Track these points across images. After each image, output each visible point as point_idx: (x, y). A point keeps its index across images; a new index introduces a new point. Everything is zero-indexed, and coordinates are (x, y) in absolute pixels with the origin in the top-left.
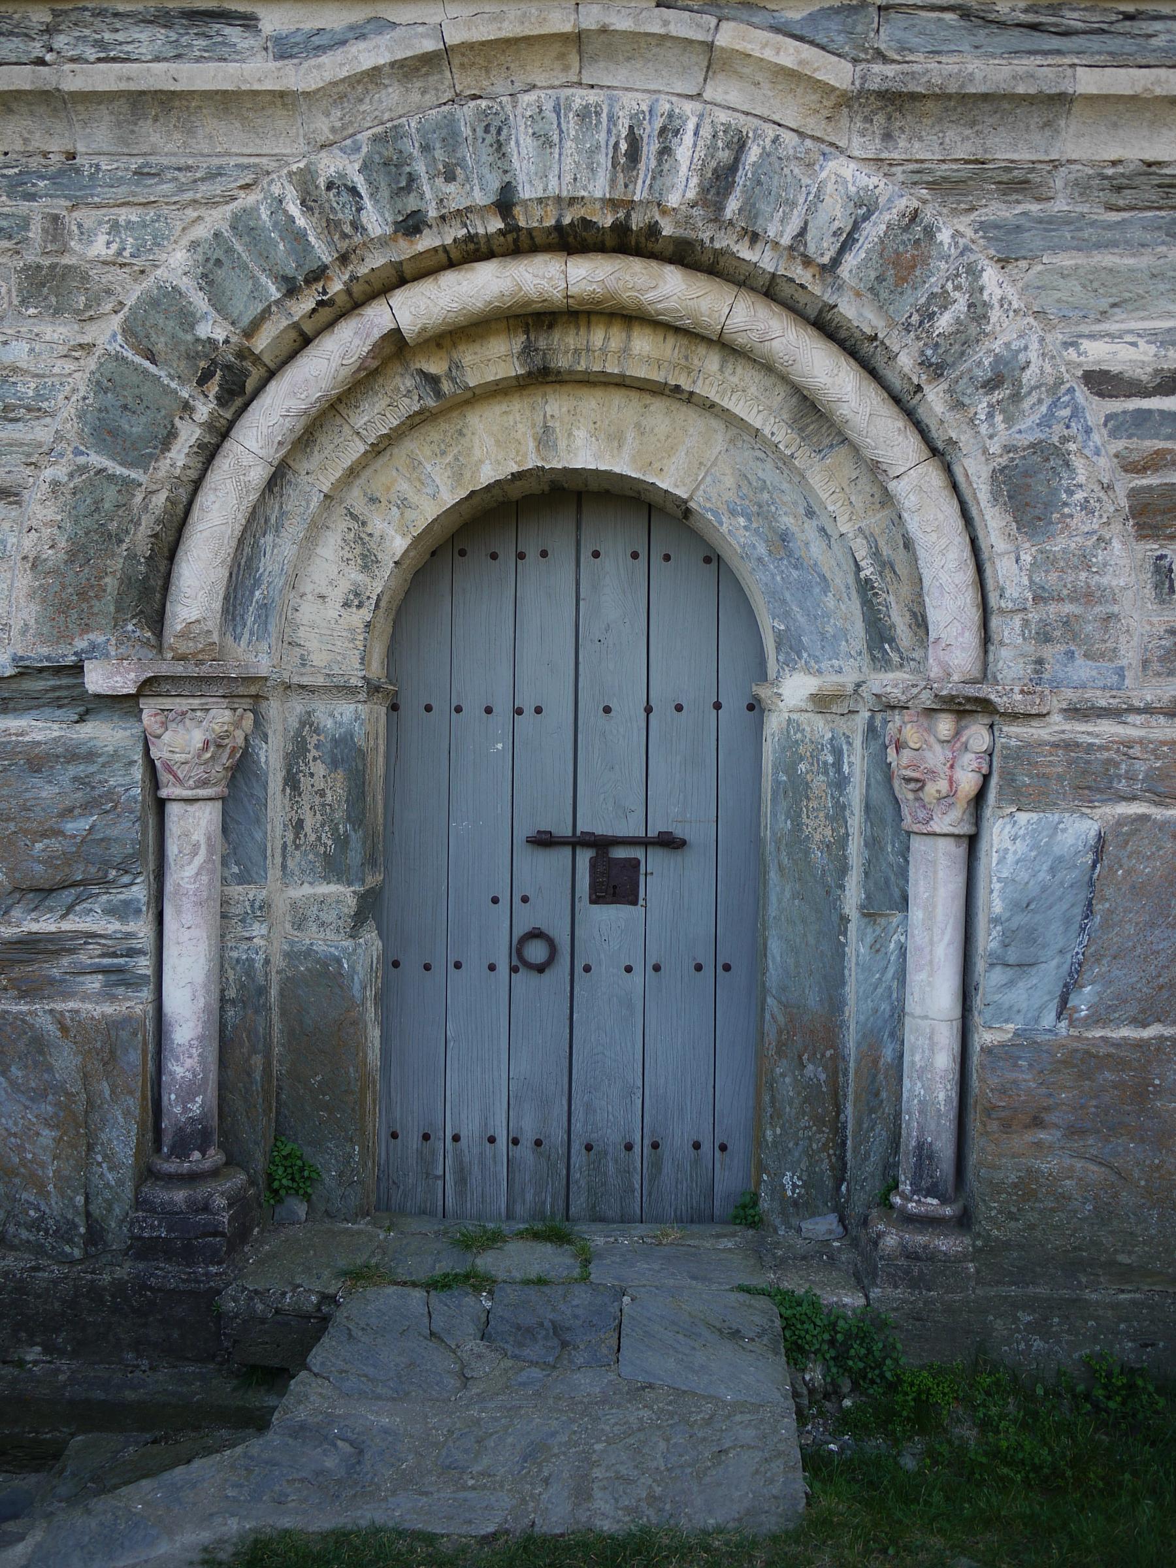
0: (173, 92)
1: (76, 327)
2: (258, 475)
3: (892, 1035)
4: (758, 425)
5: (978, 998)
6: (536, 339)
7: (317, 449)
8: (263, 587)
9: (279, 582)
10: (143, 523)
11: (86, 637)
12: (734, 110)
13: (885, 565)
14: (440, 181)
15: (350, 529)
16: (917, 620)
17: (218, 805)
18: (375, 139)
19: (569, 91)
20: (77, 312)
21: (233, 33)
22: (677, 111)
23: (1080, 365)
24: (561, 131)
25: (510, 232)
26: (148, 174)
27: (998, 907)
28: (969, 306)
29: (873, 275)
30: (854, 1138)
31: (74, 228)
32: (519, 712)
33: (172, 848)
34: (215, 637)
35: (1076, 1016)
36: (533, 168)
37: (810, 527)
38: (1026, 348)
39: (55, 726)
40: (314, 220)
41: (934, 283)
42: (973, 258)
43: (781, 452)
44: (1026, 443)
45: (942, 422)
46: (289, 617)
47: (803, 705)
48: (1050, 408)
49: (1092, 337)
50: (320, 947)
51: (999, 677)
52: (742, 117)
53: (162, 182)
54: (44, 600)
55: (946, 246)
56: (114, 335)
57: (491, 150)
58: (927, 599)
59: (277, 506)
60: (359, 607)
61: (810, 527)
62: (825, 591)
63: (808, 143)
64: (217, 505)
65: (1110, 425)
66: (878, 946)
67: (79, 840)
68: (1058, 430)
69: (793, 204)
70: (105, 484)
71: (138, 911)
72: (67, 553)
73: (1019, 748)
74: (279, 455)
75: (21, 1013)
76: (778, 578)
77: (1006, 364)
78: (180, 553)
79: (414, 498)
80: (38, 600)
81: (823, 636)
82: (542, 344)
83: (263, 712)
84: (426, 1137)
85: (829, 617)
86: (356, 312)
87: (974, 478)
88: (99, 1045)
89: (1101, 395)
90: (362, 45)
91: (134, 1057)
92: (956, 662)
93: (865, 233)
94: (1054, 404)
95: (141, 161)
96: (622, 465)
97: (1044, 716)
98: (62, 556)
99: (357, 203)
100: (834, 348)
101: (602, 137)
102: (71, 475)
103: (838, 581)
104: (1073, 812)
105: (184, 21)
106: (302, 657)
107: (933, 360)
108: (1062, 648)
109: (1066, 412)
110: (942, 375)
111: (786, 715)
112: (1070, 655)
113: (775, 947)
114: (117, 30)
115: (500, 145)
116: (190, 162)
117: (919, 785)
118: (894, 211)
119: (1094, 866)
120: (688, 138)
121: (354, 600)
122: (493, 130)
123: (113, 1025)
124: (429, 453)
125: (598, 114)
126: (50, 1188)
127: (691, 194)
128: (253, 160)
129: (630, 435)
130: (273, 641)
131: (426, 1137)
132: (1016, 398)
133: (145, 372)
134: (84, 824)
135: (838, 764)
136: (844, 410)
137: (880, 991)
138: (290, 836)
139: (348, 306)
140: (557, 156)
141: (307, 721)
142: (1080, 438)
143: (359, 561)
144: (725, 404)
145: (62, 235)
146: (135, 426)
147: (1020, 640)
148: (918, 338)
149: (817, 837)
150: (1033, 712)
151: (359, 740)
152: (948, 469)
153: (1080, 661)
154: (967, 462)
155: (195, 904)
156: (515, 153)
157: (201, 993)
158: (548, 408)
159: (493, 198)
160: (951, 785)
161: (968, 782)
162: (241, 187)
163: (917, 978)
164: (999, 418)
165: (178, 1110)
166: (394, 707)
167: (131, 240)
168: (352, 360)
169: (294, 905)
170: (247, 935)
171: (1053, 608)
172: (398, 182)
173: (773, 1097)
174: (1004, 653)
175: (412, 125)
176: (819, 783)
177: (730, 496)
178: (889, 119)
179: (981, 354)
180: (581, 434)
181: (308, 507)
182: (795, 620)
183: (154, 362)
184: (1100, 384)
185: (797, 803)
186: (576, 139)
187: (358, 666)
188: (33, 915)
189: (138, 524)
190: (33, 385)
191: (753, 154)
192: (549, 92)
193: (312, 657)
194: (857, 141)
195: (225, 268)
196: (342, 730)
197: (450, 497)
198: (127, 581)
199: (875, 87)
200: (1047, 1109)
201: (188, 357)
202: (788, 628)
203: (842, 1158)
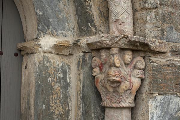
16: (101, 14)
47: (50, 50)
81: (59, 20)
85: (61, 12)
92: (127, 30)
97: (164, 53)
104: (175, 95)
117: (118, 84)
135: (65, 78)
147: (155, 21)
149: (57, 112)
150: (163, 51)
160: (130, 85)
161: (136, 82)
171: (166, 8)
176: (57, 86)
182: (47, 11)
185: (48, 96)
202: (43, 14)
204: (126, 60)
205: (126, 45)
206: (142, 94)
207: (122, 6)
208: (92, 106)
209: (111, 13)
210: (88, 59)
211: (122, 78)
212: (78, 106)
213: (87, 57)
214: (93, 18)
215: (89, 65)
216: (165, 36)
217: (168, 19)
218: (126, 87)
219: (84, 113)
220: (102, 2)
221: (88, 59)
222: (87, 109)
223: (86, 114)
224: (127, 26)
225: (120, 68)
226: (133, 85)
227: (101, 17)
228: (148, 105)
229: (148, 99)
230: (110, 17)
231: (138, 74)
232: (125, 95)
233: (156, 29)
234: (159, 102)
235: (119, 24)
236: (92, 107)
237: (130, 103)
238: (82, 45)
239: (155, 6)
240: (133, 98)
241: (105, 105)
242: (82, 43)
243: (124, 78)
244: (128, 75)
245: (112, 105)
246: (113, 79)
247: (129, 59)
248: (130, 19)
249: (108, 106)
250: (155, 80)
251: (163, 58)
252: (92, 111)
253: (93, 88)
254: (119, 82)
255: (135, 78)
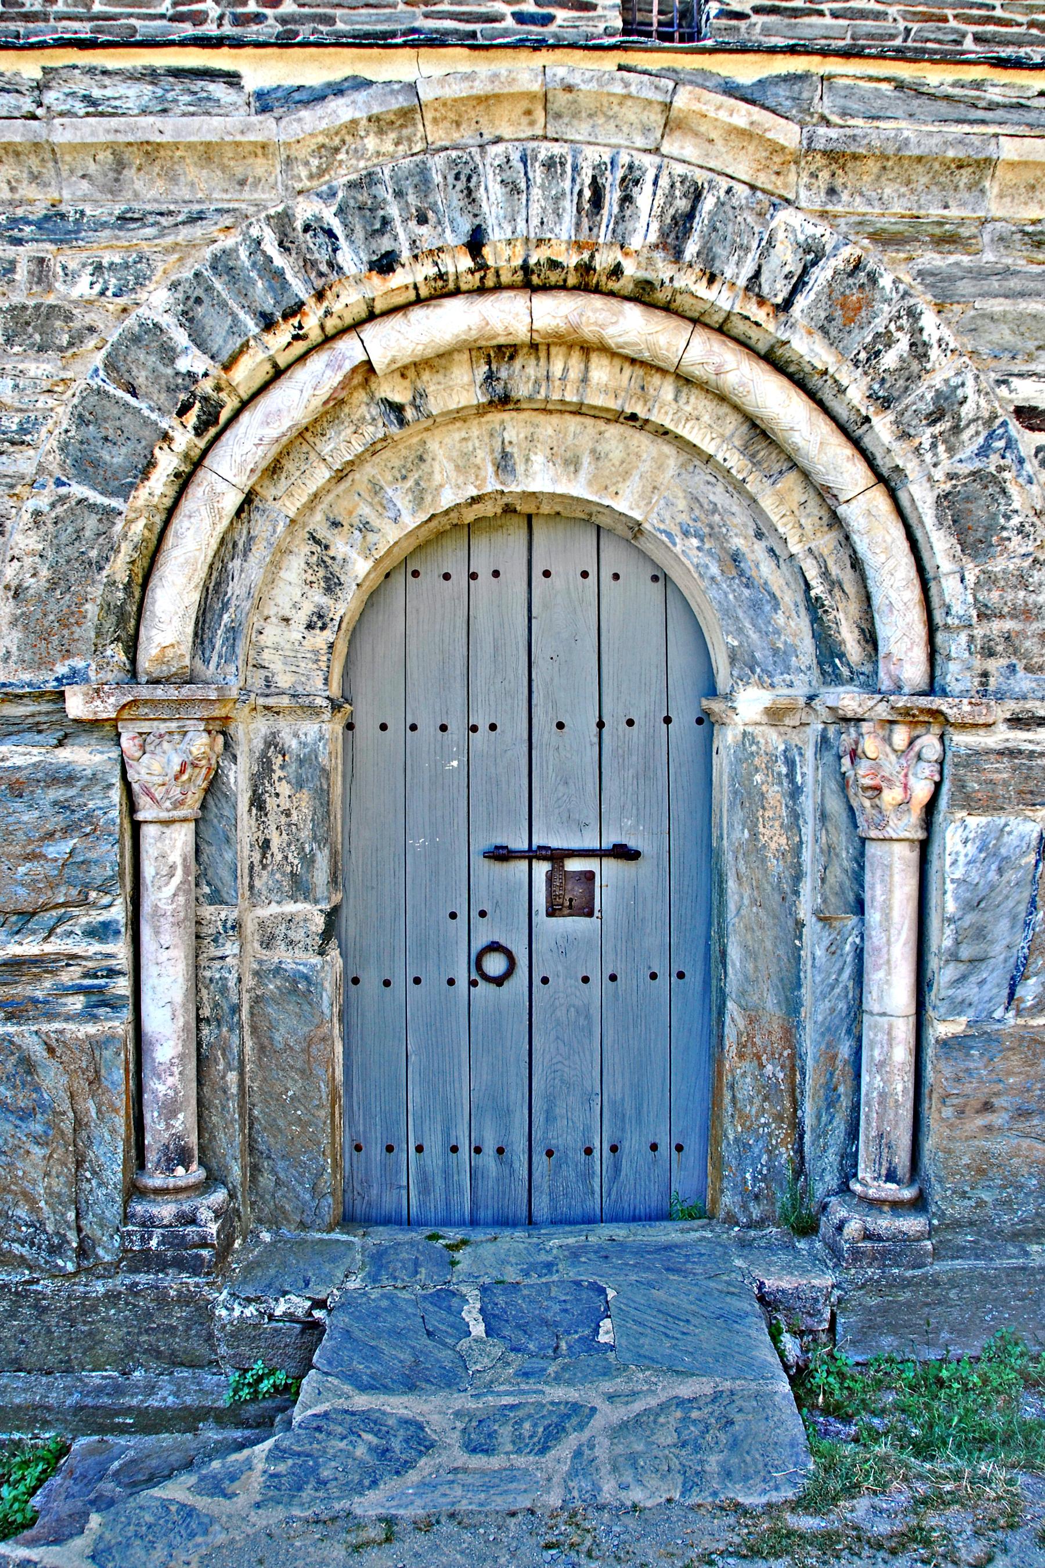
0: (158, 144)
1: (59, 363)
2: (232, 500)
3: (849, 1032)
4: (711, 450)
5: (933, 994)
6: (498, 369)
7: (284, 475)
8: (232, 610)
9: (246, 605)
10: (123, 549)
11: (67, 662)
12: (689, 163)
13: (834, 584)
14: (413, 224)
15: (313, 553)
17: (192, 825)
18: (351, 185)
19: (534, 144)
20: (61, 349)
21: (218, 90)
22: (637, 163)
23: (1011, 401)
24: (528, 180)
25: (479, 270)
26: (132, 219)
27: (951, 907)
28: (911, 345)
29: (823, 315)
30: (813, 1130)
31: (59, 270)
32: (474, 729)
33: (148, 870)
34: (187, 661)
35: (1022, 1006)
36: (502, 212)
37: (760, 547)
38: (963, 385)
39: (35, 751)
40: (292, 260)
41: (879, 324)
42: (912, 301)
43: (733, 477)
44: (967, 471)
45: (889, 451)
46: (254, 639)
47: (758, 718)
48: (986, 439)
49: (1020, 375)
50: (289, 966)
51: (948, 689)
52: (698, 170)
53: (145, 226)
54: (26, 627)
55: (888, 291)
56: (97, 370)
57: (461, 196)
58: (876, 616)
59: (245, 532)
60: (322, 628)
61: (760, 547)
62: (776, 607)
63: (759, 194)
64: (192, 531)
65: (1041, 455)
66: (833, 948)
67: (60, 862)
68: (994, 460)
69: (747, 249)
70: (86, 513)
71: (119, 932)
72: (48, 581)
73: (969, 756)
74: (250, 483)
75: (8, 1034)
76: (731, 596)
77: (946, 399)
78: (154, 581)
79: (375, 522)
80: (20, 627)
81: (776, 651)
82: (503, 374)
83: (232, 732)
84: (390, 1149)
86: (327, 346)
87: (919, 504)
88: (84, 1065)
89: (1032, 429)
90: (341, 101)
91: (119, 1075)
93: (813, 277)
94: (990, 436)
95: (123, 208)
96: (578, 488)
97: (990, 725)
98: (44, 584)
99: (333, 244)
100: (785, 382)
101: (567, 184)
102: (53, 506)
103: (787, 599)
105: (171, 79)
106: (267, 679)
107: (881, 394)
108: (1004, 662)
109: (1001, 444)
110: (888, 407)
111: (741, 728)
112: (1012, 668)
113: (734, 953)
114: (105, 87)
115: (469, 192)
116: (172, 207)
118: (840, 258)
119: (1036, 865)
120: (648, 186)
121: (318, 621)
122: (463, 178)
123: (95, 1044)
124: (390, 478)
125: (562, 164)
126: (42, 1204)
127: (653, 237)
128: (231, 206)
129: (586, 460)
130: (240, 663)
131: (390, 1149)
132: (956, 430)
133: (126, 405)
134: (66, 846)
136: (797, 439)
137: (837, 991)
138: (257, 856)
139: (320, 340)
140: (524, 202)
141: (272, 742)
142: (1014, 468)
143: (323, 584)
144: (679, 431)
145: (47, 276)
146: (116, 457)
147: (967, 655)
148: (866, 373)
149: (773, 846)
150: (981, 722)
151: (324, 760)
152: (893, 494)
153: (1021, 673)
154: (914, 489)
155: (173, 924)
156: (485, 198)
157: (180, 1012)
158: (506, 435)
159: (465, 239)
161: (922, 791)
162: (220, 230)
163: (874, 977)
164: (941, 448)
165: (162, 1126)
166: (350, 726)
167: (113, 281)
168: (324, 393)
169: (262, 925)
170: (220, 954)
171: (997, 626)
172: (372, 225)
173: (734, 1096)
174: (953, 667)
175: (387, 171)
176: (775, 793)
177: (684, 518)
178: (833, 175)
179: (923, 389)
180: (538, 459)
181: (274, 532)
183: (134, 395)
184: (1030, 419)
186: (542, 187)
187: (322, 687)
188: (17, 937)
189: (118, 551)
190: (16, 420)
191: (708, 204)
192: (517, 144)
193: (276, 678)
194: (803, 193)
195: (204, 305)
196: (307, 750)
197: (411, 521)
198: (107, 607)
199: (821, 147)
200: (997, 1094)
201: (168, 389)
202: (741, 645)
203: (800, 1151)
213: (832, 730)
216: (991, 688)
217: (1000, 648)
219: (825, 848)
224: (907, 666)
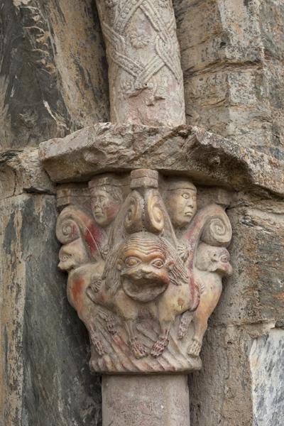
117: (157, 292)
147: (253, 100)
160: (193, 293)
204: (180, 213)
205: (183, 159)
206: (224, 326)
207: (155, 50)
208: (55, 374)
209: (117, 71)
210: (42, 214)
211: (170, 271)
212: (9, 377)
214: (58, 85)
215: (47, 236)
218: (180, 301)
219: (31, 397)
220: (84, 42)
221: (42, 214)
222: (41, 386)
223: (37, 402)
224: (170, 110)
225: (162, 238)
226: (201, 296)
227: (82, 87)
228: (247, 360)
229: (246, 341)
230: (114, 85)
231: (216, 258)
232: (176, 328)
233: (260, 125)
234: (277, 353)
235: (147, 103)
236: (58, 378)
237: (192, 356)
238: (25, 165)
239: (251, 56)
240: (199, 338)
241: (109, 366)
242: (23, 162)
243: (175, 269)
244: (184, 261)
245: (132, 363)
246: (142, 272)
247: (189, 209)
248: (179, 90)
249: (119, 368)
250: (266, 278)
251: (279, 214)
252: (57, 390)
253: (60, 312)
254: (160, 283)
255: (206, 272)
